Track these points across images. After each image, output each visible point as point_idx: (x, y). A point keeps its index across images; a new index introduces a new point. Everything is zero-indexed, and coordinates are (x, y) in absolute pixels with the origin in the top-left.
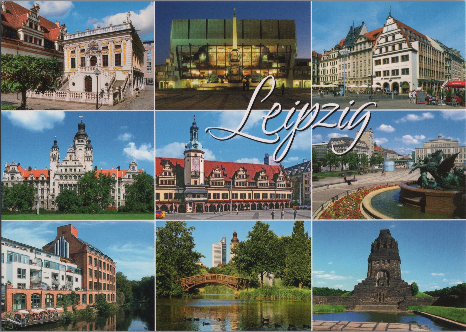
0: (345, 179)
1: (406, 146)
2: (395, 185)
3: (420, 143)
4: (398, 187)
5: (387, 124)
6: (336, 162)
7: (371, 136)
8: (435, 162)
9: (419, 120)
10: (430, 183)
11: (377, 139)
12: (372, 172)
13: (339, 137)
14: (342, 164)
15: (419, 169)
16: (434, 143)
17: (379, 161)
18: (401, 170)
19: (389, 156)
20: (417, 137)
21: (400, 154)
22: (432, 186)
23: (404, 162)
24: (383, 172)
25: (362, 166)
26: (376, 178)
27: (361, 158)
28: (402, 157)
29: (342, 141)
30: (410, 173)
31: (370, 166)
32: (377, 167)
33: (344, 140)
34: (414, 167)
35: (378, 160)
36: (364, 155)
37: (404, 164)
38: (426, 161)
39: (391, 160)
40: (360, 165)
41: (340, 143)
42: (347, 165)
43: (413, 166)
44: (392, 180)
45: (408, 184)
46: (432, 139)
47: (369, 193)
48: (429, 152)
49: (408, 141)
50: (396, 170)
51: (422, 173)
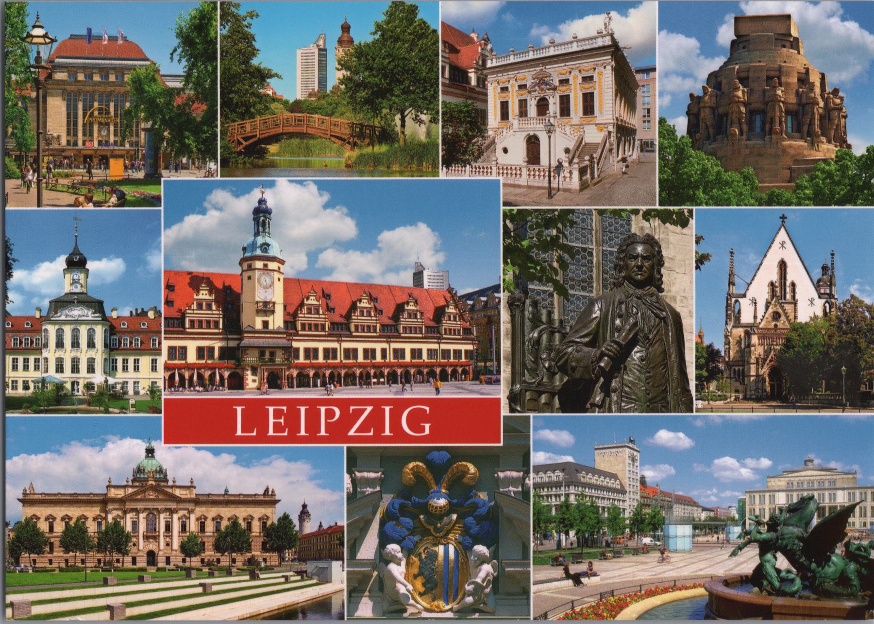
0: (566, 570)
1: (723, 486)
3: (757, 477)
6: (542, 525)
7: (633, 460)
8: (797, 526)
11: (647, 467)
12: (636, 552)
13: (549, 462)
14: (559, 533)
15: (756, 545)
16: (795, 478)
17: (654, 525)
18: (707, 546)
19: (679, 511)
20: (750, 462)
23: (716, 527)
24: (662, 553)
27: (606, 515)
28: (712, 514)
29: (558, 473)
30: (734, 554)
31: (631, 537)
32: (647, 540)
33: (563, 470)
34: (742, 541)
35: (650, 522)
36: (616, 508)
37: (717, 533)
38: (773, 524)
39: (683, 521)
40: (604, 533)
41: (554, 478)
42: (572, 533)
43: (739, 537)
46: (788, 467)
48: (782, 499)
49: (728, 473)
50: (697, 546)
51: (762, 554)
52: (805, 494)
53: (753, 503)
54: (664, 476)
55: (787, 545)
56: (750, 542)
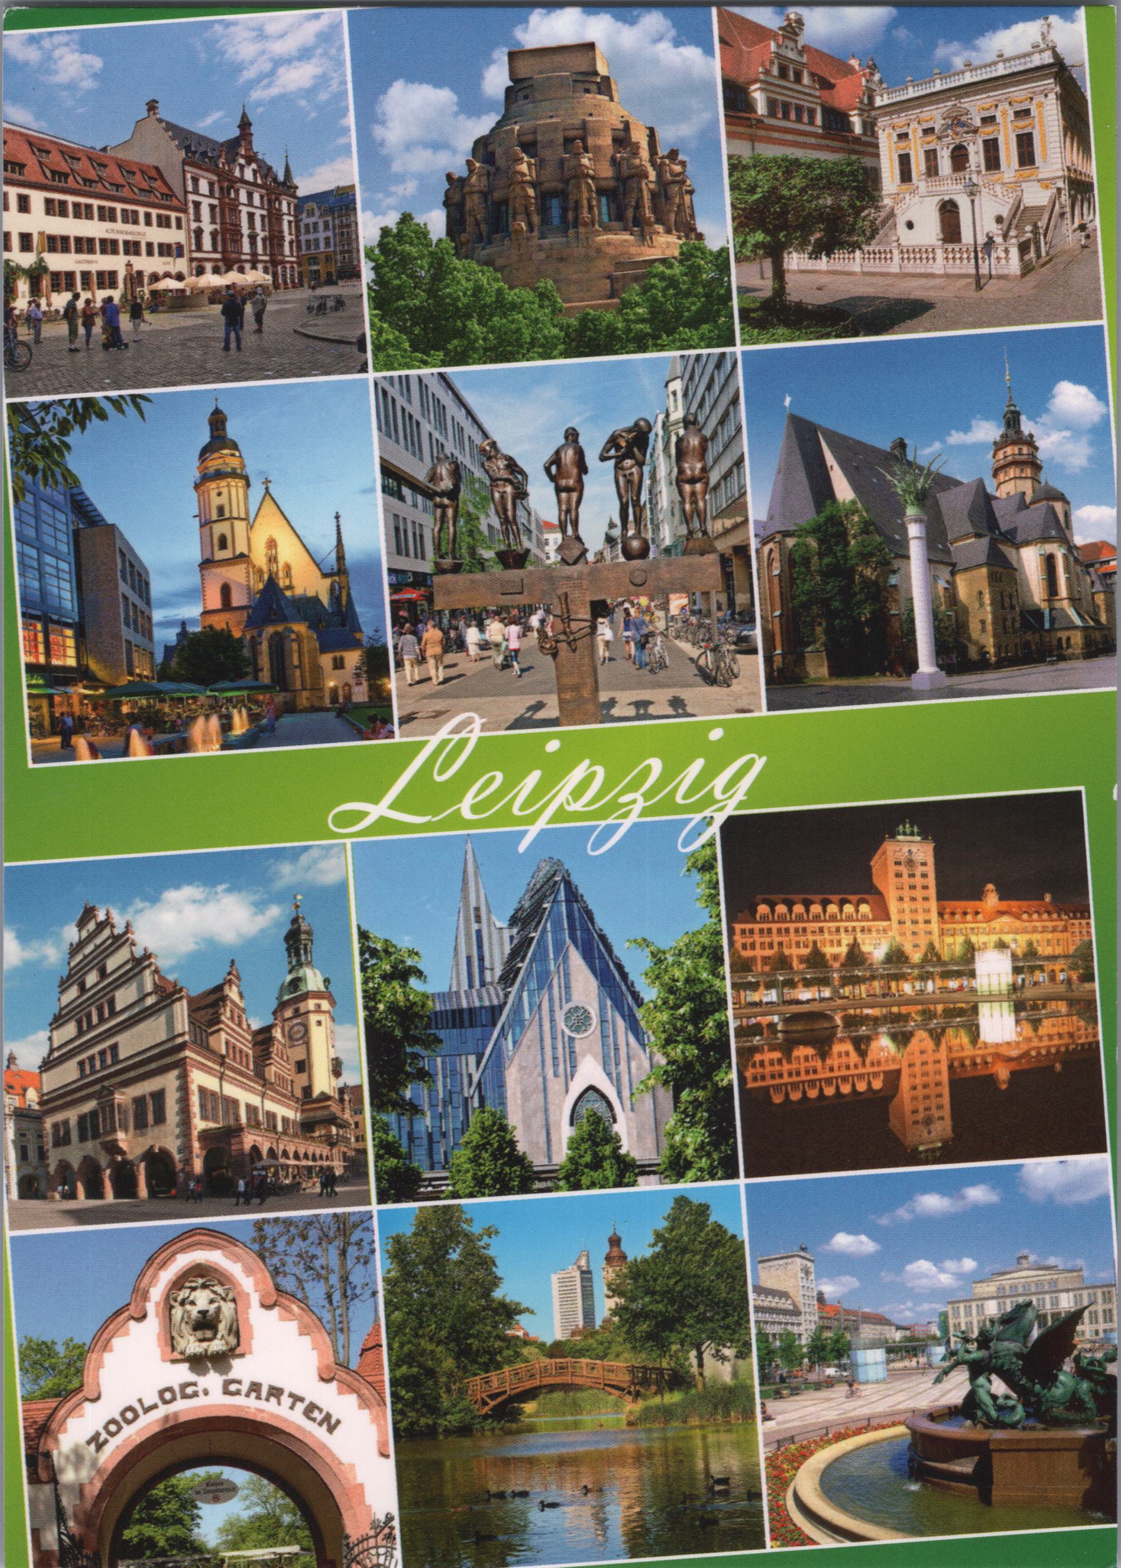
1: (919, 1298)
2: (894, 1424)
3: (961, 1283)
4: (901, 1429)
5: (853, 1231)
7: (807, 1272)
8: (1014, 1341)
9: (953, 1210)
10: (1000, 1409)
12: (818, 1386)
15: (965, 1367)
16: (1006, 1281)
17: (838, 1351)
18: (906, 1372)
19: (868, 1332)
20: (950, 1265)
21: (904, 1324)
22: (1008, 1419)
23: (914, 1349)
25: (784, 1372)
26: (826, 1405)
27: (778, 1343)
28: (908, 1333)
30: (938, 1380)
31: (811, 1369)
32: (831, 1371)
35: (833, 1349)
37: (916, 1355)
38: (984, 1340)
39: (873, 1345)
43: (944, 1359)
44: (882, 1407)
45: (932, 1417)
46: (997, 1267)
47: (812, 1453)
48: (992, 1309)
51: (973, 1378)
52: (1021, 1300)
53: (957, 1315)
54: (845, 1290)
55: (1002, 1365)
56: (957, 1364)
